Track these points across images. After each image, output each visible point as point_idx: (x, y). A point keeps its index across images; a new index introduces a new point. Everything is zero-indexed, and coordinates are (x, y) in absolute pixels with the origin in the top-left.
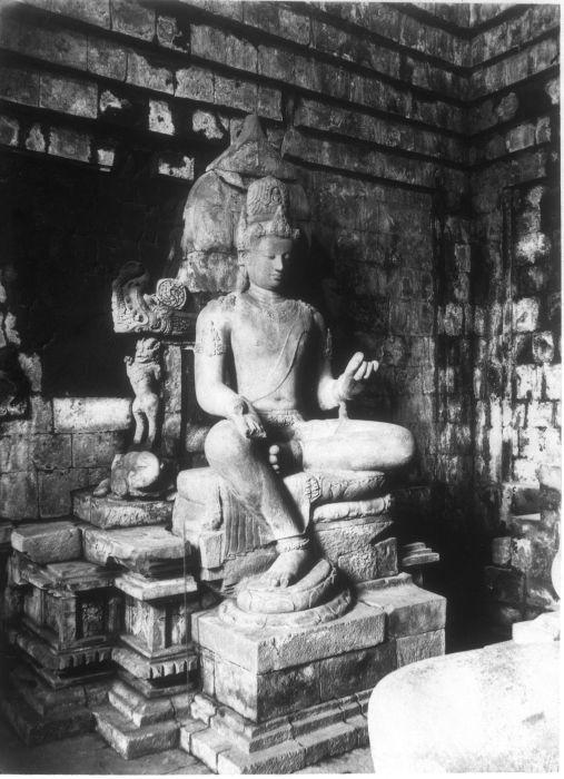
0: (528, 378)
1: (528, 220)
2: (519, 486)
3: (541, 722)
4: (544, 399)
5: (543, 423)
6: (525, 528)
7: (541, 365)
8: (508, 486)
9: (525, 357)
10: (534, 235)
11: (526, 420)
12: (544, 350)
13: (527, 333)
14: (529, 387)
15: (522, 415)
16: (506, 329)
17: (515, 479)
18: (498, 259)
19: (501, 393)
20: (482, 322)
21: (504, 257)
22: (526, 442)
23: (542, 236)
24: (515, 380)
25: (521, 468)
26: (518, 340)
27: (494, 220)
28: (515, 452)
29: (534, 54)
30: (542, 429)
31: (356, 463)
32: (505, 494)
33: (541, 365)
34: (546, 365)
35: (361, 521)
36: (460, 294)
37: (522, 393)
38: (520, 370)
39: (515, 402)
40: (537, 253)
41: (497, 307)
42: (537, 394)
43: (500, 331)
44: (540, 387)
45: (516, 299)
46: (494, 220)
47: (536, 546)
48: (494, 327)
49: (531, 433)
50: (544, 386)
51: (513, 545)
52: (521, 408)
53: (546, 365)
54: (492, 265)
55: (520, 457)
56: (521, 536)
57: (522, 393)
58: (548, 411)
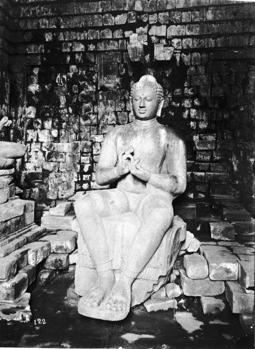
0: (31, 135)
1: (33, 78)
2: (28, 172)
3: (140, 185)
4: (37, 141)
5: (37, 150)
6: (36, 184)
7: (37, 130)
8: (24, 172)
9: (31, 127)
10: (35, 84)
11: (30, 149)
12: (38, 125)
13: (32, 118)
14: (32, 137)
15: (29, 147)
16: (23, 116)
17: (26, 170)
18: (21, 91)
19: (21, 139)
20: (14, 113)
21: (24, 90)
22: (30, 156)
23: (38, 86)
24: (27, 134)
25: (28, 166)
26: (28, 121)
27: (20, 76)
28: (26, 160)
29: (40, 21)
30: (37, 152)
31: (8, 155)
32: (23, 175)
33: (37, 130)
34: (39, 130)
35: (7, 176)
36: (7, 102)
37: (29, 139)
38: (28, 131)
39: (26, 143)
40: (36, 91)
41: (20, 108)
42: (35, 140)
43: (21, 117)
44: (36, 137)
45: (28, 106)
46: (20, 76)
47: (40, 190)
48: (19, 115)
49: (32, 154)
50: (38, 137)
51: (31, 191)
52: (28, 145)
53: (39, 130)
54: (19, 93)
55: (28, 162)
56: (35, 187)
57: (29, 139)
58: (39, 146)
